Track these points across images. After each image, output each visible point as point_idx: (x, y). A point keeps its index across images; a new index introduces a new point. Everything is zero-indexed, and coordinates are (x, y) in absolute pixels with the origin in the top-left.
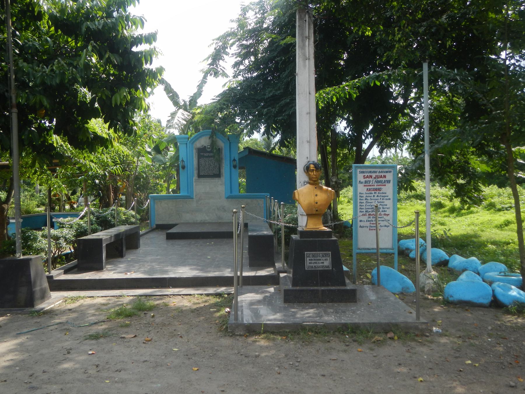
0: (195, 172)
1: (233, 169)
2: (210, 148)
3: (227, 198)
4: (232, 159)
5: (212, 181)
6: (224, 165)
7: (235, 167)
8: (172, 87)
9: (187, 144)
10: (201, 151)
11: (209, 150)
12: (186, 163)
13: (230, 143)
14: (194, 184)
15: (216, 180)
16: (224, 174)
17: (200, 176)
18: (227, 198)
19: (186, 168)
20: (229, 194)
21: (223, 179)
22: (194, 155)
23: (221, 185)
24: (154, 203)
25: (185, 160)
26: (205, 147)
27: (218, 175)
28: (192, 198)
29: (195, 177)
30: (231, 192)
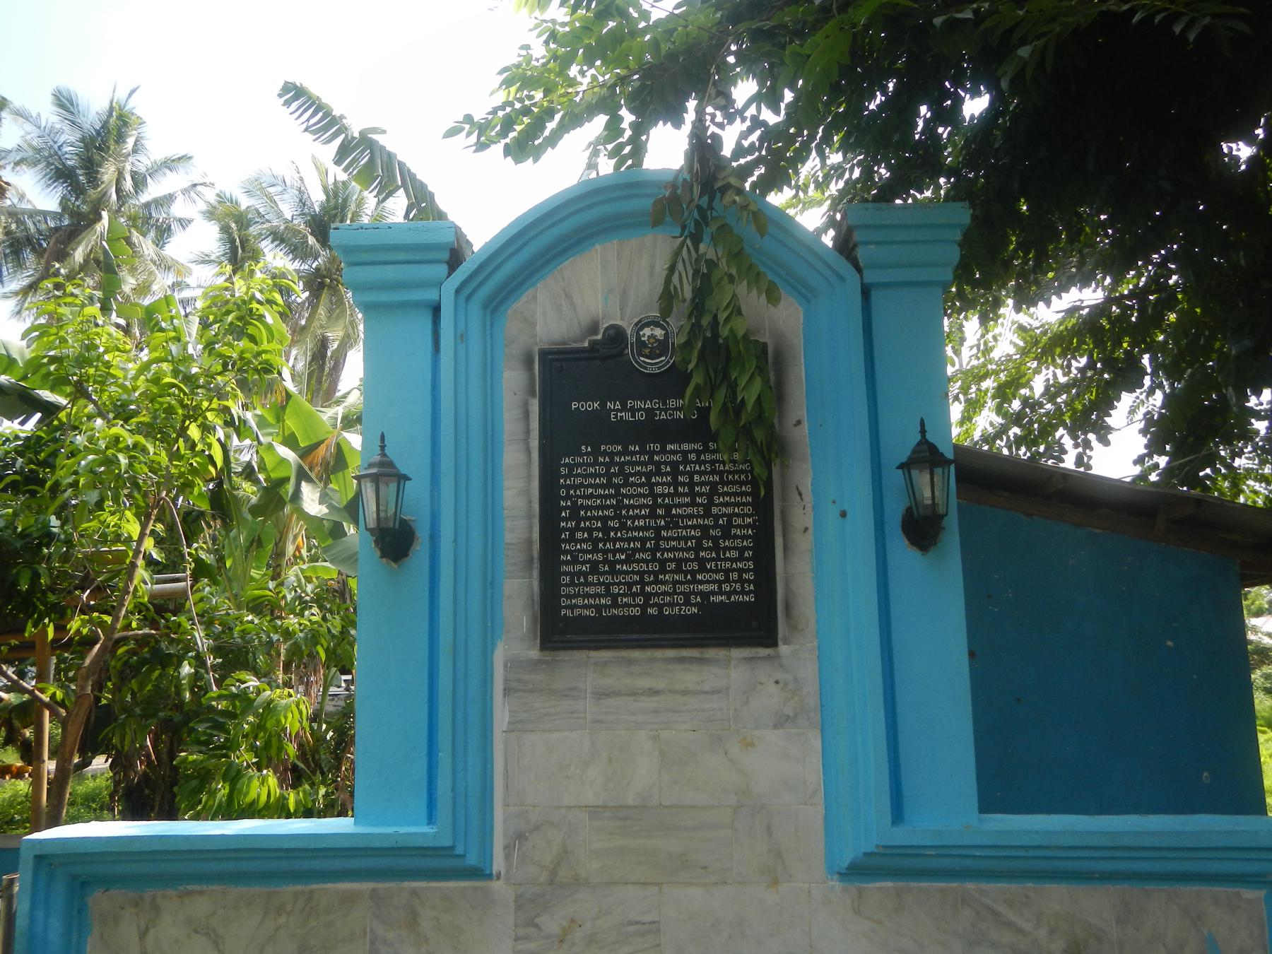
0: (517, 593)
1: (903, 553)
2: (662, 347)
3: (858, 871)
4: (901, 444)
5: (689, 677)
6: (801, 516)
7: (921, 529)
8: (442, 203)
9: (436, 310)
10: (583, 388)
11: (653, 365)
12: (416, 491)
13: (866, 292)
14: (501, 716)
15: (728, 672)
16: (807, 608)
17: (559, 630)
18: (859, 871)
19: (420, 549)
20: (871, 830)
21: (797, 654)
22: (509, 423)
23: (782, 721)
24: (77, 918)
25: (412, 461)
26: (616, 336)
27: (752, 621)
28: (479, 873)
29: (515, 638)
30: (898, 814)
